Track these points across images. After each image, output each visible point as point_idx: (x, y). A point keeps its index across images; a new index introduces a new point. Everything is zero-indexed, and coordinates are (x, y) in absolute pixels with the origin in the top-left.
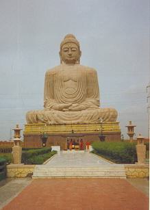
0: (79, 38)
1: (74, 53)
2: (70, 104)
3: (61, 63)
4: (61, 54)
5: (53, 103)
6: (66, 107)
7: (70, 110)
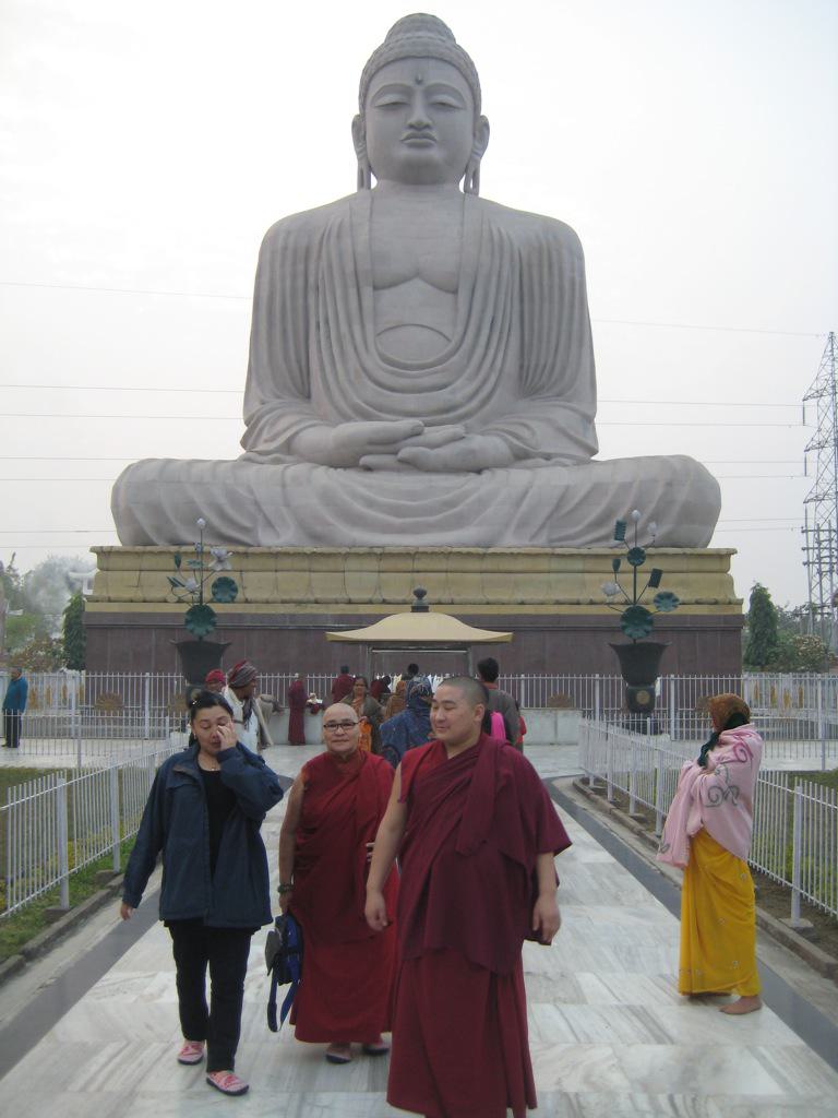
0: (467, 38)
1: (441, 117)
2: (406, 424)
3: (363, 181)
4: (359, 128)
5: (288, 422)
6: (388, 444)
7: (413, 465)
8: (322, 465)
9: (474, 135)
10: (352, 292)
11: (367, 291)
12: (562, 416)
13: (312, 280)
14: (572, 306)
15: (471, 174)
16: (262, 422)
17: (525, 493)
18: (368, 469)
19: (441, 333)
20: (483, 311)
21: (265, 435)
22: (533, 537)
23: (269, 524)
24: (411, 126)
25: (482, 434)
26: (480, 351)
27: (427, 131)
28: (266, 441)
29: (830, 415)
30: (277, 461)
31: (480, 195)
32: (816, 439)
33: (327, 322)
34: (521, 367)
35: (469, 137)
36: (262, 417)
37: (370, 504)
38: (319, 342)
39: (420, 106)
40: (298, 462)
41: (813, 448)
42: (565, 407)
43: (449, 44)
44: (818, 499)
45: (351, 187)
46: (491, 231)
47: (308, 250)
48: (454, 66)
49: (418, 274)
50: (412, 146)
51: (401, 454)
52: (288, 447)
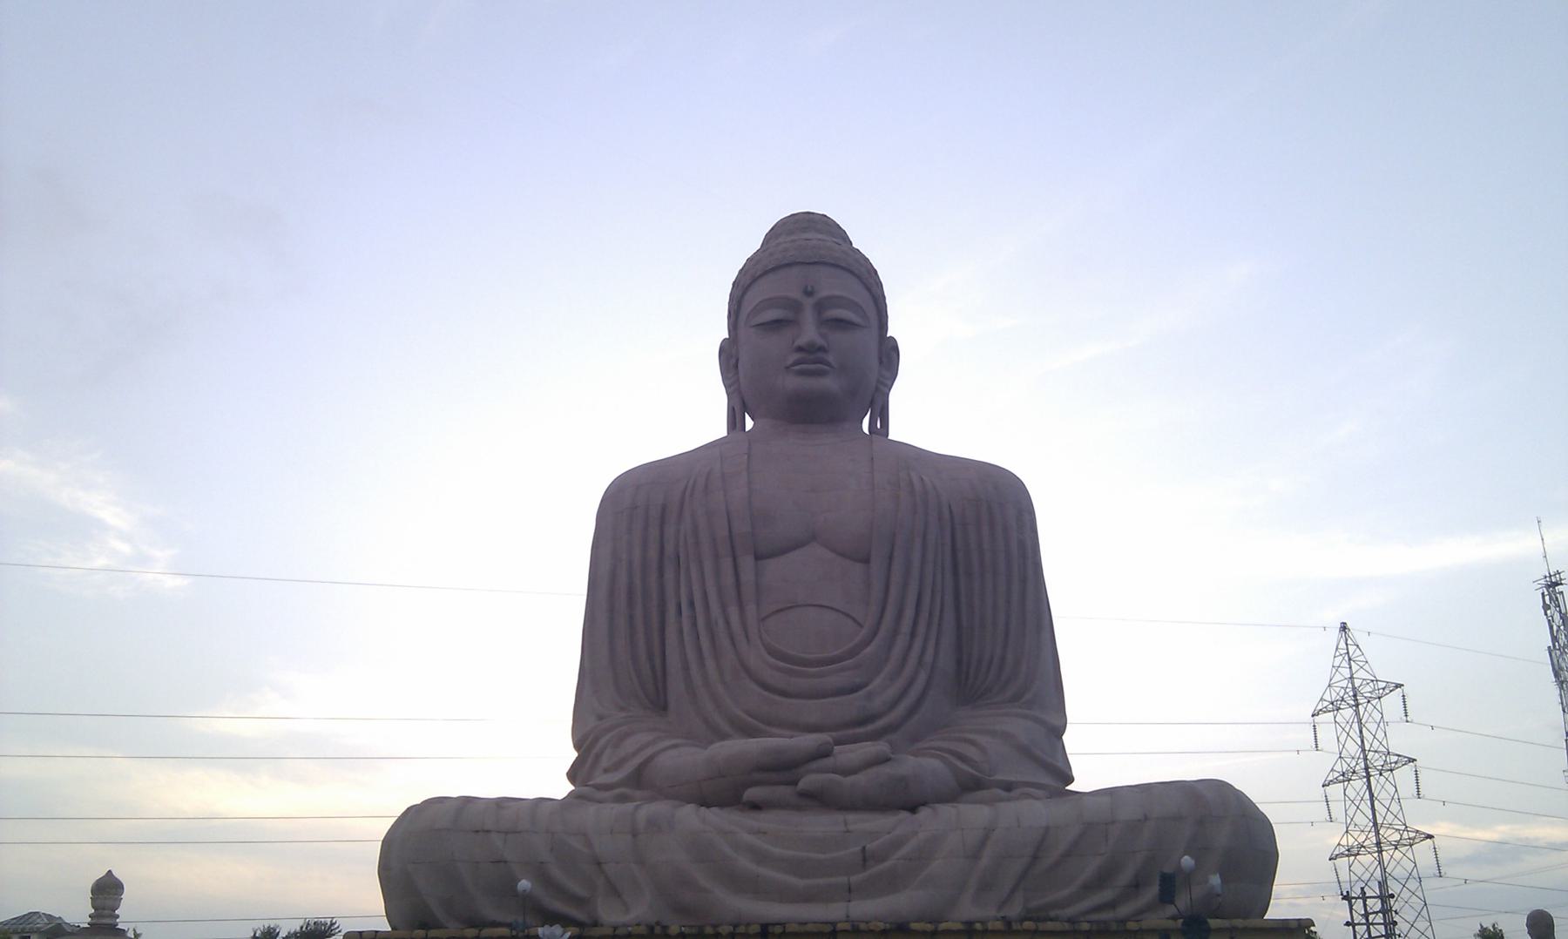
1: (839, 338)
3: (734, 421)
4: (729, 356)
6: (783, 768)
7: (820, 800)
8: (688, 800)
9: (881, 362)
10: (727, 564)
11: (747, 562)
12: (1019, 727)
13: (669, 549)
14: (1024, 581)
15: (878, 411)
16: (602, 741)
17: (983, 843)
18: (756, 807)
19: (848, 615)
20: (905, 585)
21: (605, 762)
22: (1002, 904)
23: (614, 891)
24: (800, 349)
25: (915, 755)
26: (901, 642)
27: (820, 355)
28: (606, 771)
29: (1355, 735)
30: (622, 799)
31: (891, 437)
32: (1338, 768)
33: (692, 604)
34: (959, 662)
35: (875, 362)
36: (596, 740)
37: (761, 857)
38: (681, 631)
39: (809, 322)
40: (652, 799)
41: (1335, 781)
42: (1026, 717)
43: (845, 247)
44: (1351, 852)
45: (717, 428)
46: (911, 483)
47: (664, 509)
48: (852, 272)
49: (812, 538)
50: (802, 373)
51: (802, 785)
52: (638, 779)
